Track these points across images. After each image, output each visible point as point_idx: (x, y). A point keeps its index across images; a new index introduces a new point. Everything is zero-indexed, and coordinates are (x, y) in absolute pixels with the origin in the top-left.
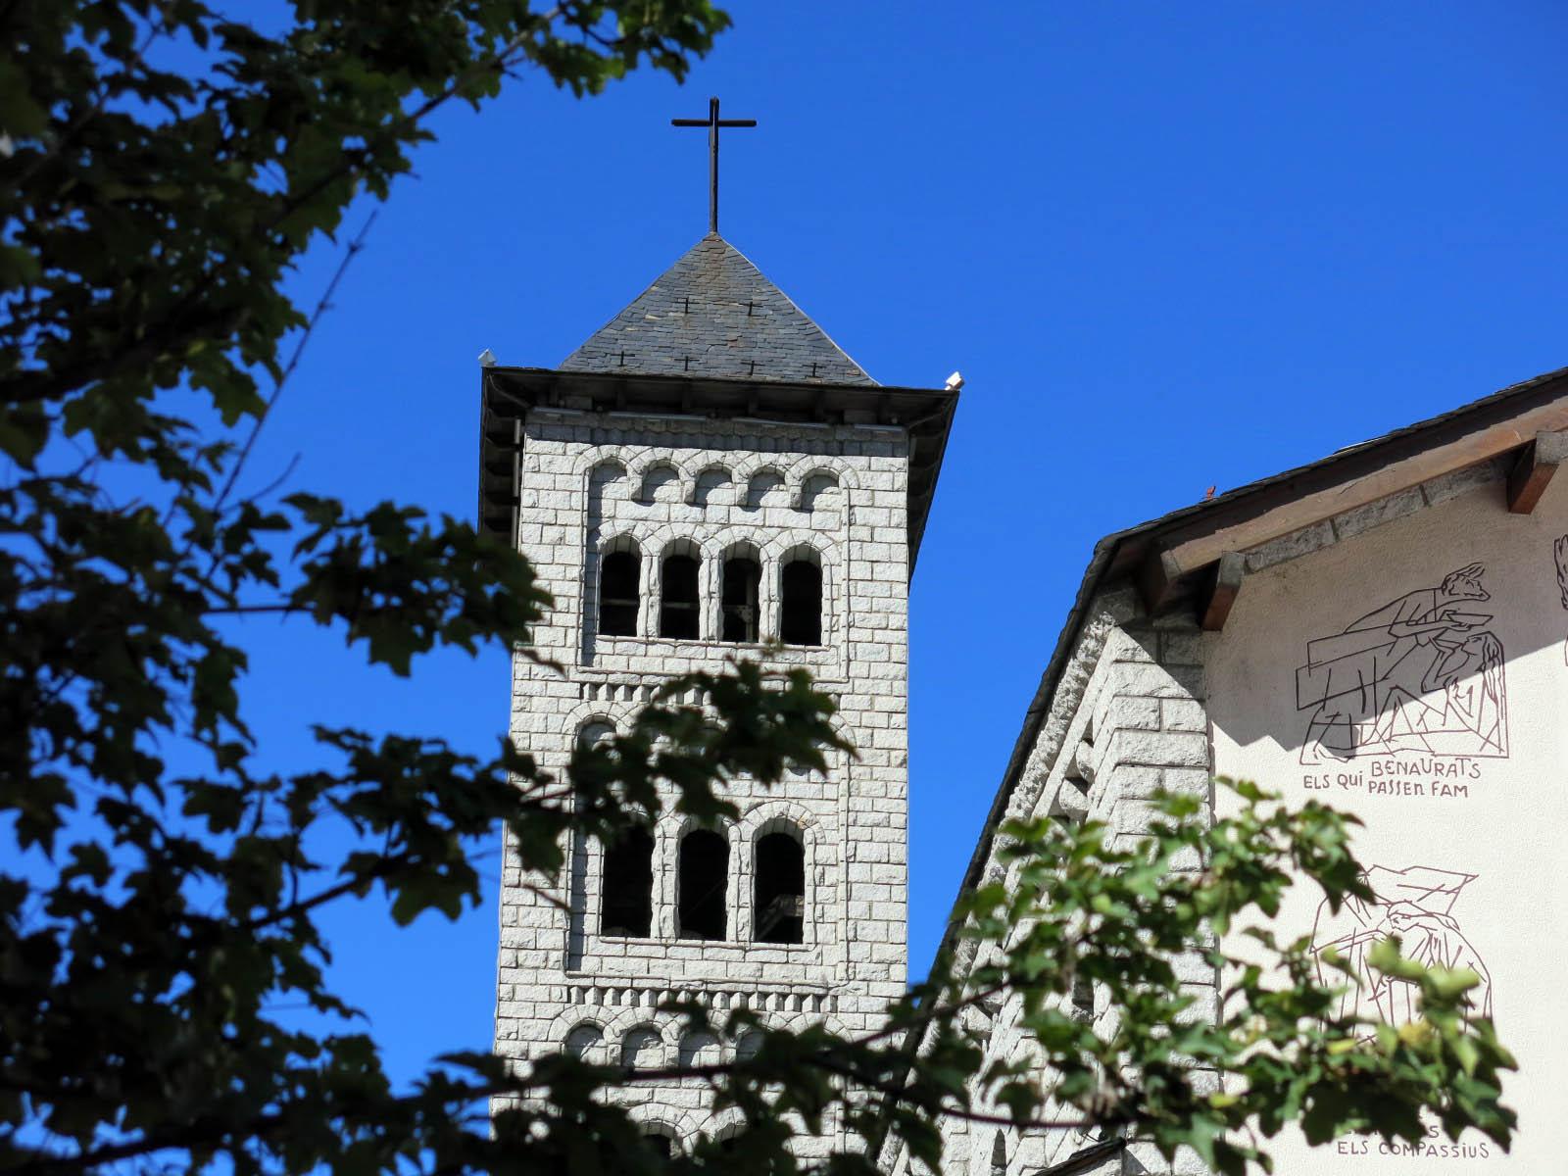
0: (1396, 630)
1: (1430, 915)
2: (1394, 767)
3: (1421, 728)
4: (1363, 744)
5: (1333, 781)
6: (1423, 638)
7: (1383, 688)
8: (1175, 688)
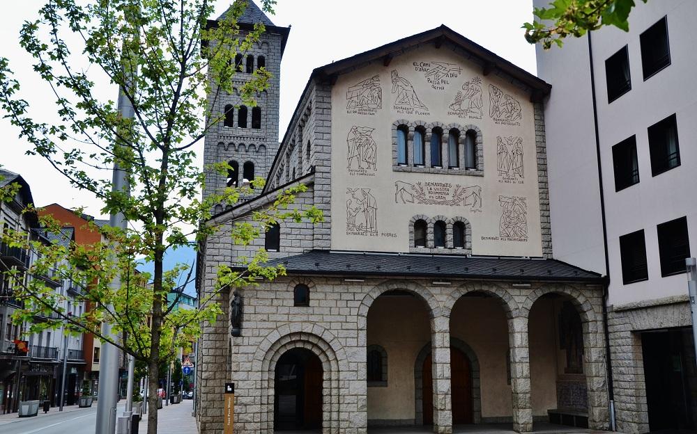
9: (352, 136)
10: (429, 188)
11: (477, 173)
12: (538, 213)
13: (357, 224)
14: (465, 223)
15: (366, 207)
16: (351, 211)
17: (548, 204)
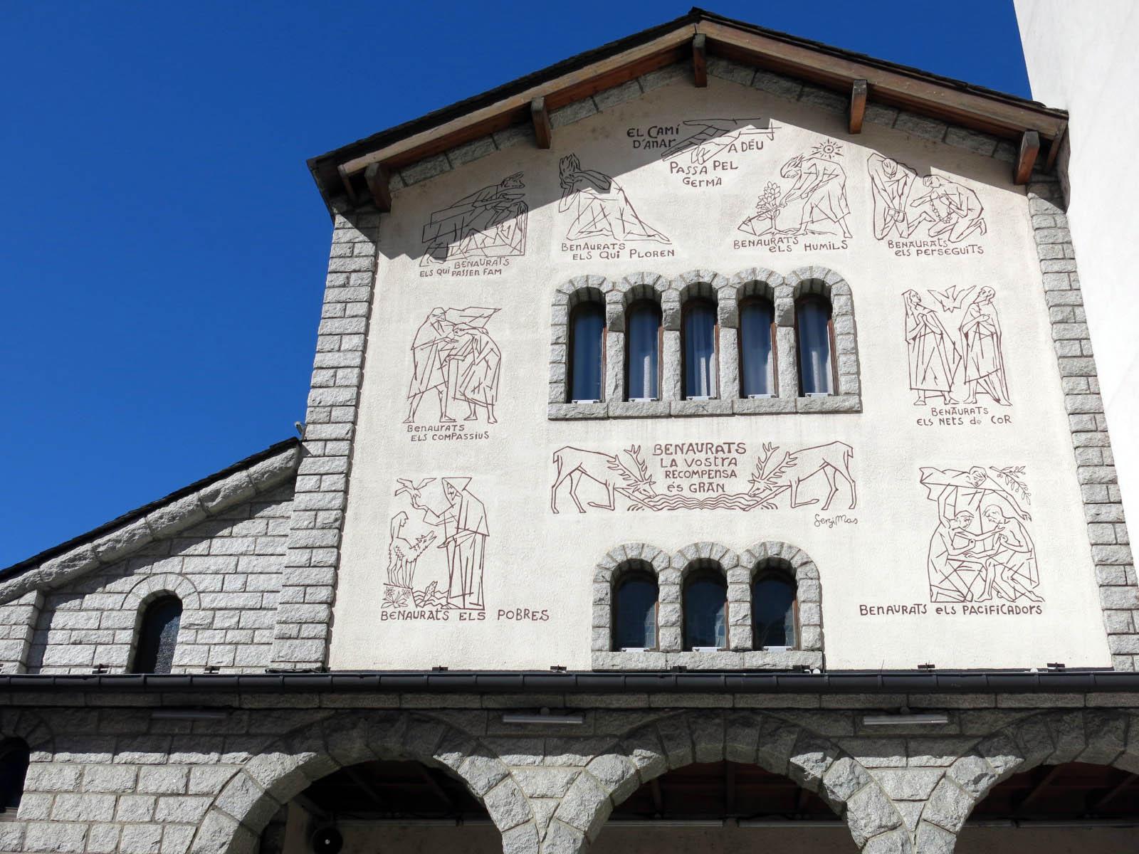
0: (476, 204)
1: (474, 328)
2: (466, 264)
3: (483, 246)
4: (452, 255)
5: (434, 272)
6: (488, 207)
7: (466, 230)
8: (362, 237)
9: (428, 334)
10: (667, 462)
11: (833, 402)
12: (1079, 515)
13: (419, 585)
14: (795, 563)
15: (451, 530)
16: (405, 549)
17: (1114, 481)
